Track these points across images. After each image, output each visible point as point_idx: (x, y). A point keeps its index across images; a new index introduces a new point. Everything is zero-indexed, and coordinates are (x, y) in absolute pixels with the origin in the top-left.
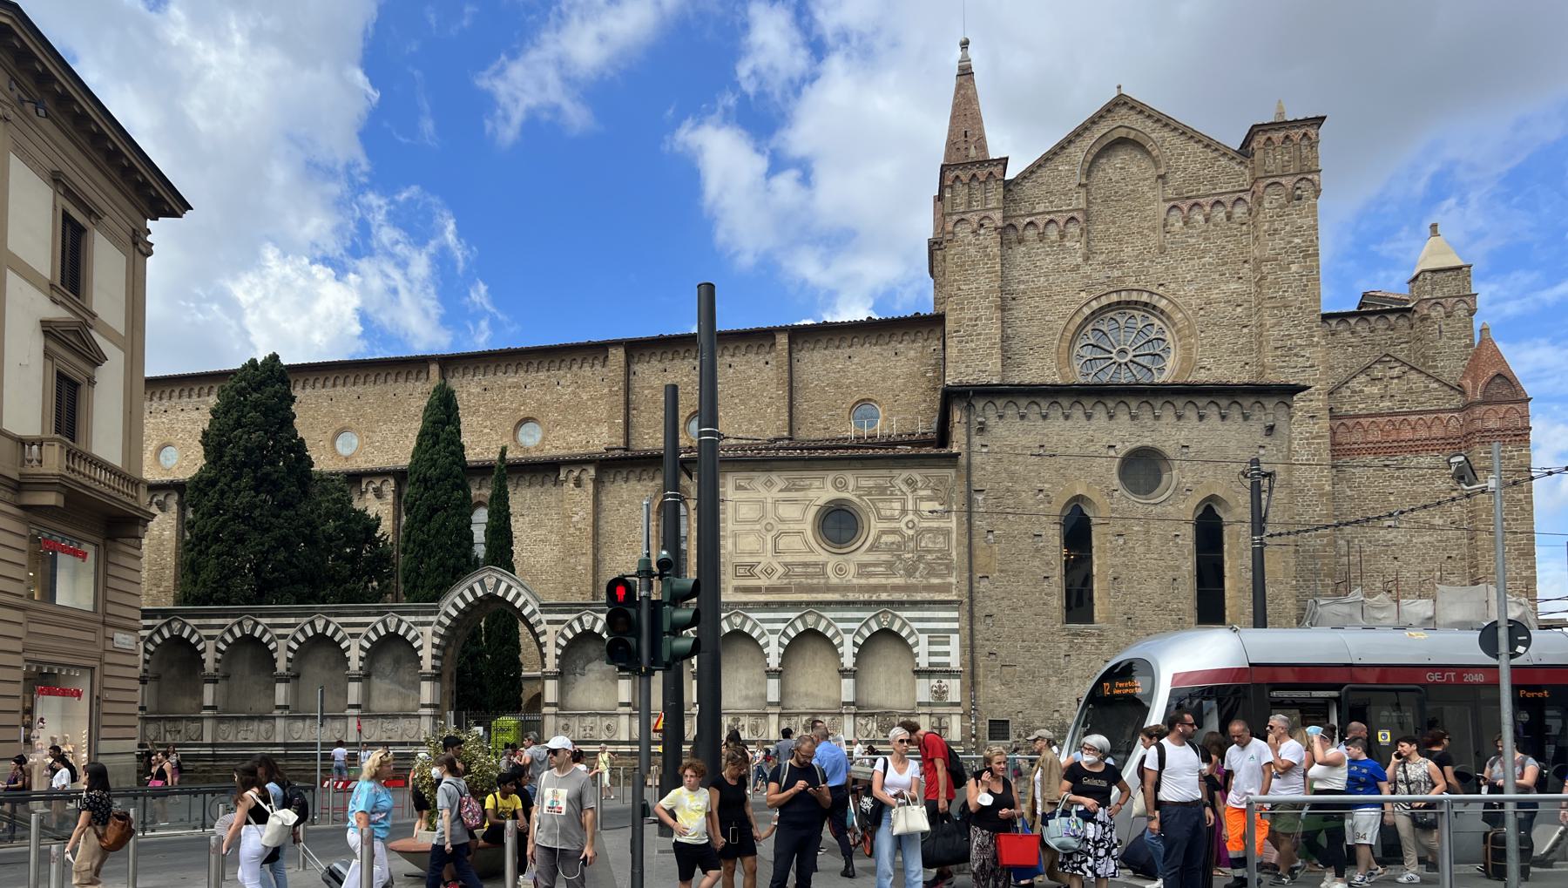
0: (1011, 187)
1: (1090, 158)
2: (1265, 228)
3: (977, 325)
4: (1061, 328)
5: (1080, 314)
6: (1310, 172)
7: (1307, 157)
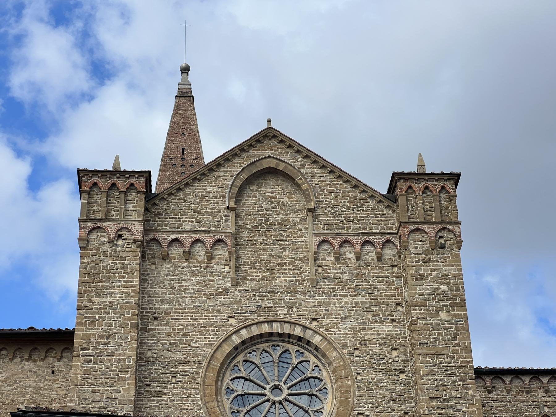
0: (157, 202)
1: (239, 183)
2: (412, 272)
3: (108, 344)
4: (208, 356)
5: (229, 342)
6: (450, 223)
7: (447, 209)
